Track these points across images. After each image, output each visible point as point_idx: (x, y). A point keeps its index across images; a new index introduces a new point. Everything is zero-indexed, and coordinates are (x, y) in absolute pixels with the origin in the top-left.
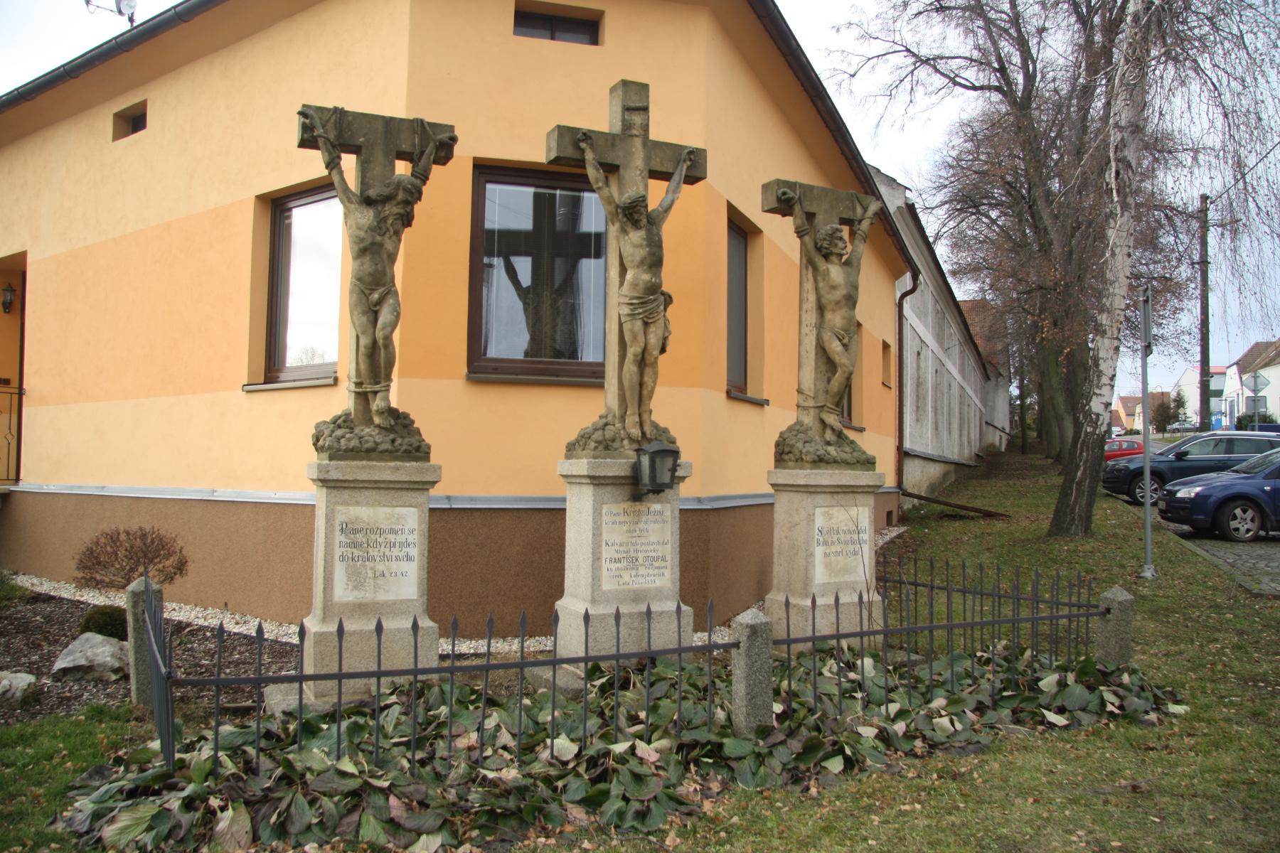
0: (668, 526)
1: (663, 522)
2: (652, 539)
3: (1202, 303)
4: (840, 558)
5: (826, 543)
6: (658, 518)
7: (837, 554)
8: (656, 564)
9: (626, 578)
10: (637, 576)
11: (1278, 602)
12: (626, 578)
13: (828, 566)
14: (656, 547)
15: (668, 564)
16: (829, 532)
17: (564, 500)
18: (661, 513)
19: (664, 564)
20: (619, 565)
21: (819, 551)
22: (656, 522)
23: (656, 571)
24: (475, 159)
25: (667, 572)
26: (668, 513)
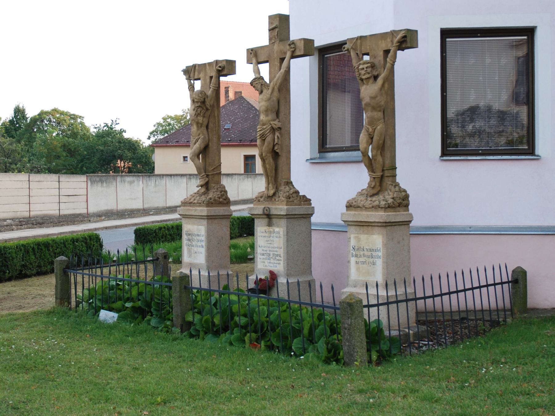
0: (282, 240)
1: (280, 237)
2: (275, 245)
3: (138, 210)
4: (365, 266)
5: (356, 256)
6: (278, 235)
7: (363, 263)
8: (277, 258)
9: (266, 264)
10: (270, 263)
11: (1, 296)
12: (266, 264)
13: (358, 269)
14: (277, 249)
15: (282, 259)
16: (358, 249)
17: (347, 210)
18: (279, 233)
19: (280, 258)
20: (263, 257)
21: (353, 260)
22: (277, 237)
23: (277, 262)
24: (441, 29)
25: (282, 262)
26: (282, 233)
